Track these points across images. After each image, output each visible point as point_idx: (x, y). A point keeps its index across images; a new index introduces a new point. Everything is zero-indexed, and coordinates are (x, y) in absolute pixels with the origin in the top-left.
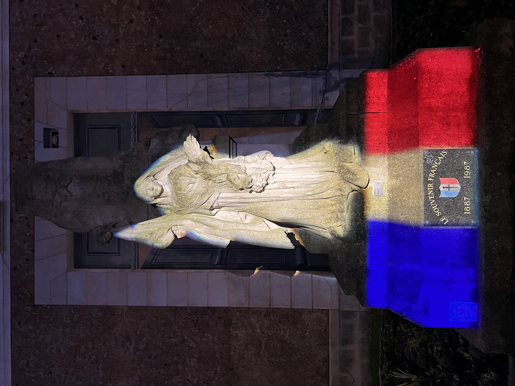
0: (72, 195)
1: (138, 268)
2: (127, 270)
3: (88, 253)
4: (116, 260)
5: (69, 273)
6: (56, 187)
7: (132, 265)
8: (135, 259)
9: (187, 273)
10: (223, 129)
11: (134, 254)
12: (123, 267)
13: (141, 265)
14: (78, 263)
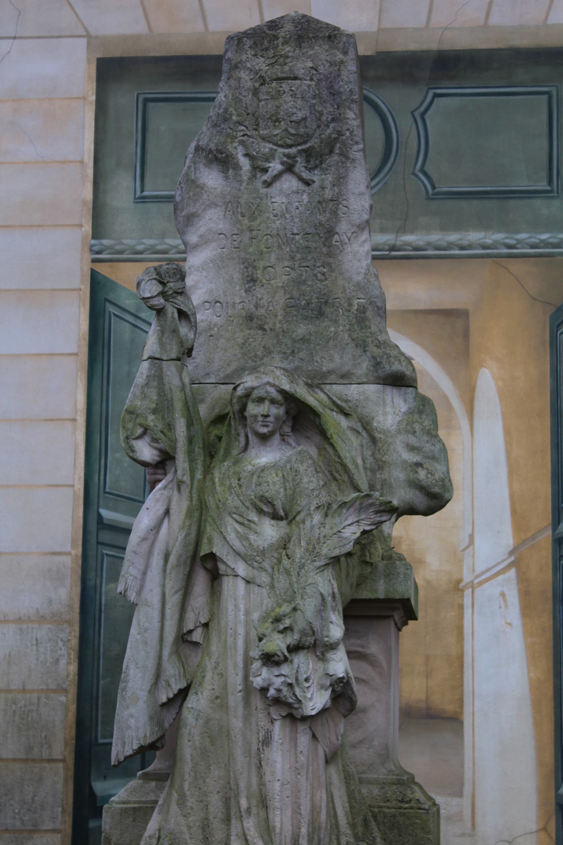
0: (268, 184)
1: (94, 261)
2: (88, 228)
3: (146, 101)
4: (122, 190)
5: (84, 41)
6: (290, 146)
7: (105, 242)
8: (121, 252)
9: (74, 420)
10: (545, 540)
11: (140, 248)
12: (99, 215)
13: (104, 270)
14: (112, 70)
